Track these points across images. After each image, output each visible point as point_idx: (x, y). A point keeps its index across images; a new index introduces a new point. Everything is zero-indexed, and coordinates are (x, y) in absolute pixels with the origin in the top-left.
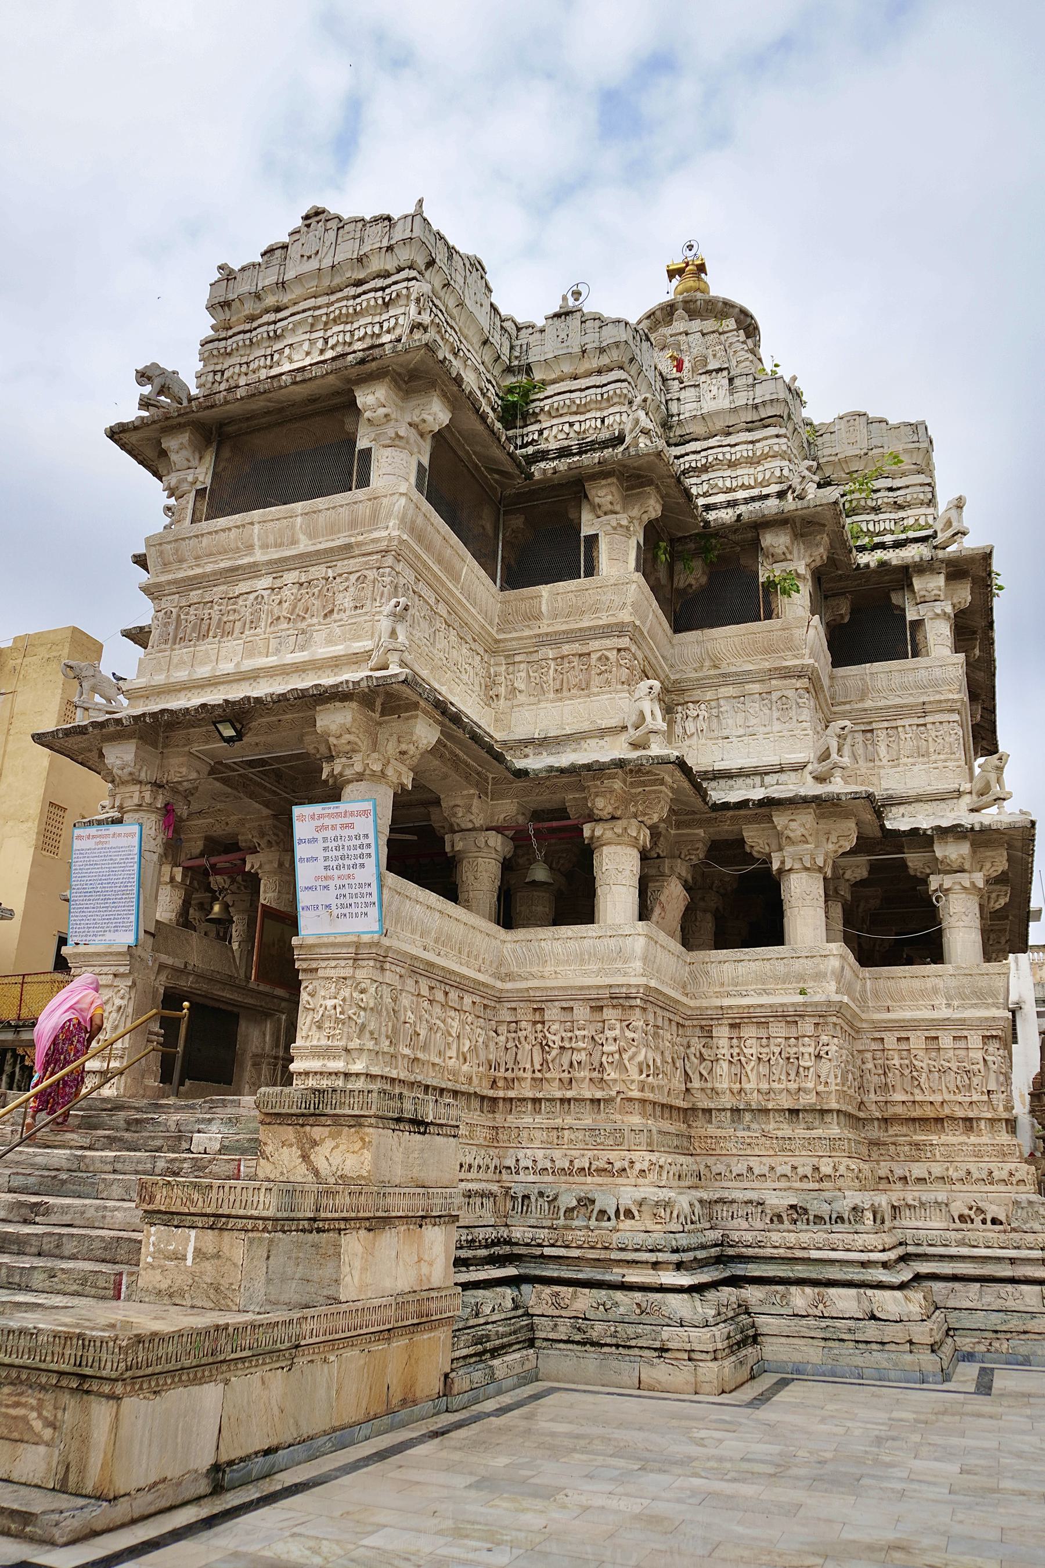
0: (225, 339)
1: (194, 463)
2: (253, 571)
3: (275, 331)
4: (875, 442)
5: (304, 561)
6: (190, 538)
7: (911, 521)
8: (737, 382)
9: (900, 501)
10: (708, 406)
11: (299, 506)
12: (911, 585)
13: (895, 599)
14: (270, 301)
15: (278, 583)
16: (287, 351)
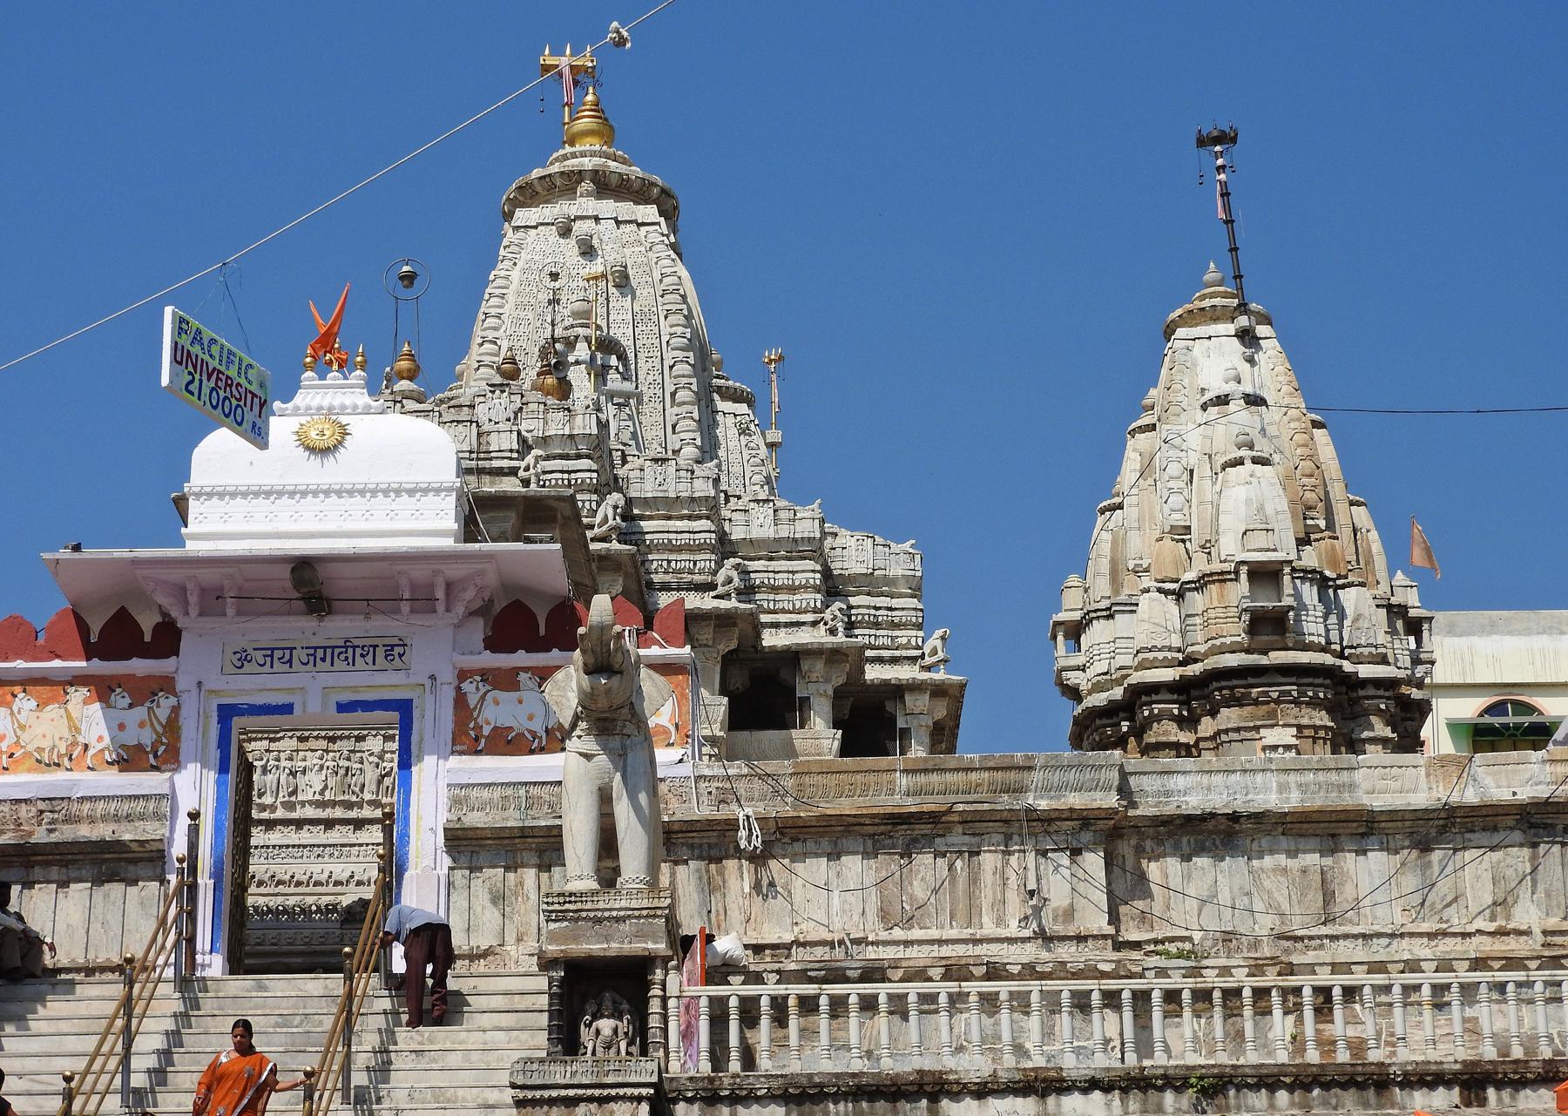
4: (879, 564)
7: (904, 640)
8: (783, 515)
9: (896, 620)
10: (756, 533)
12: (902, 698)
13: (889, 707)
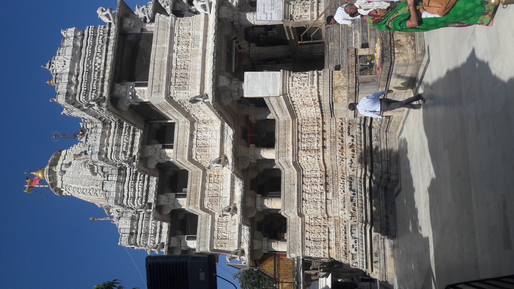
0: (81, 90)
1: (126, 86)
2: (170, 58)
3: (87, 71)
5: (171, 43)
6: (153, 82)
11: (154, 45)
14: (74, 79)
15: (176, 52)
16: (96, 64)
